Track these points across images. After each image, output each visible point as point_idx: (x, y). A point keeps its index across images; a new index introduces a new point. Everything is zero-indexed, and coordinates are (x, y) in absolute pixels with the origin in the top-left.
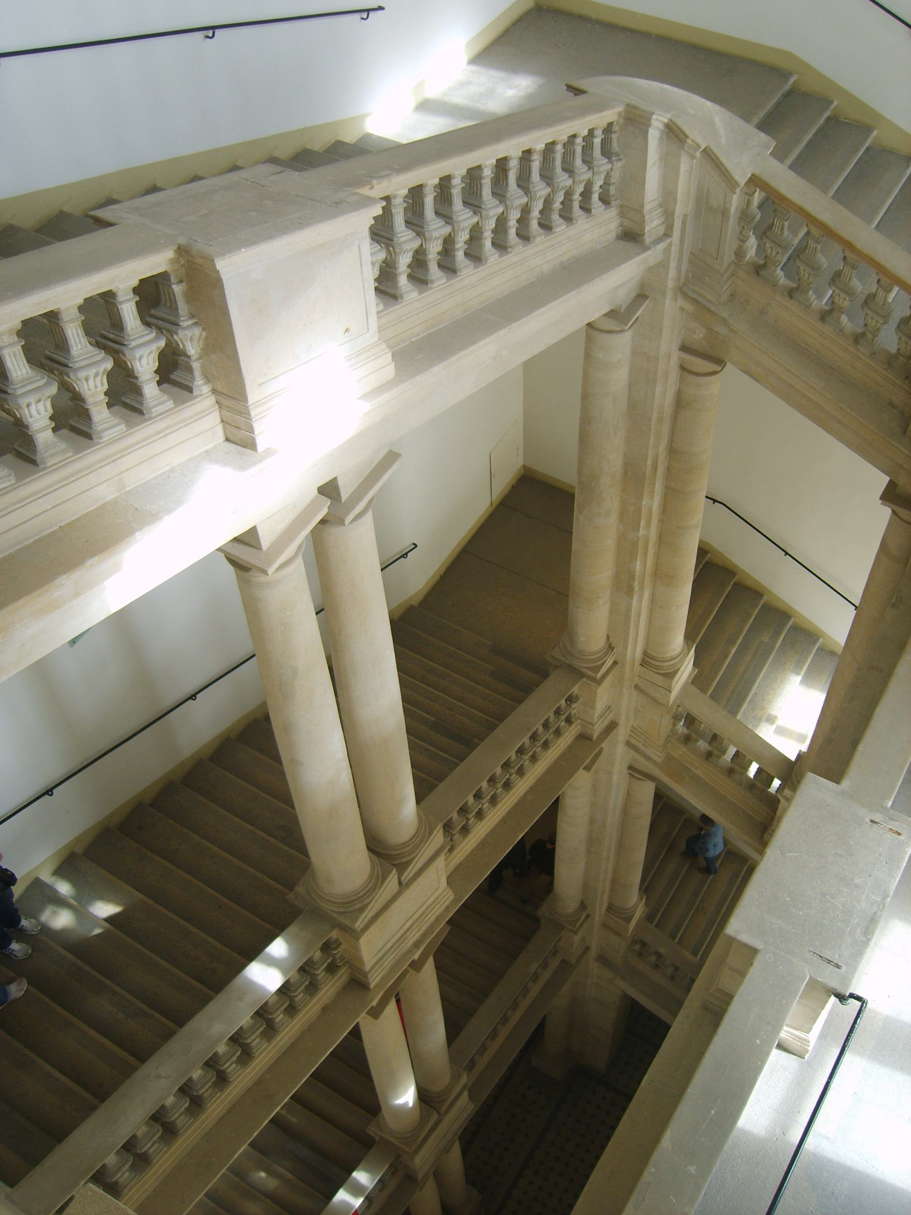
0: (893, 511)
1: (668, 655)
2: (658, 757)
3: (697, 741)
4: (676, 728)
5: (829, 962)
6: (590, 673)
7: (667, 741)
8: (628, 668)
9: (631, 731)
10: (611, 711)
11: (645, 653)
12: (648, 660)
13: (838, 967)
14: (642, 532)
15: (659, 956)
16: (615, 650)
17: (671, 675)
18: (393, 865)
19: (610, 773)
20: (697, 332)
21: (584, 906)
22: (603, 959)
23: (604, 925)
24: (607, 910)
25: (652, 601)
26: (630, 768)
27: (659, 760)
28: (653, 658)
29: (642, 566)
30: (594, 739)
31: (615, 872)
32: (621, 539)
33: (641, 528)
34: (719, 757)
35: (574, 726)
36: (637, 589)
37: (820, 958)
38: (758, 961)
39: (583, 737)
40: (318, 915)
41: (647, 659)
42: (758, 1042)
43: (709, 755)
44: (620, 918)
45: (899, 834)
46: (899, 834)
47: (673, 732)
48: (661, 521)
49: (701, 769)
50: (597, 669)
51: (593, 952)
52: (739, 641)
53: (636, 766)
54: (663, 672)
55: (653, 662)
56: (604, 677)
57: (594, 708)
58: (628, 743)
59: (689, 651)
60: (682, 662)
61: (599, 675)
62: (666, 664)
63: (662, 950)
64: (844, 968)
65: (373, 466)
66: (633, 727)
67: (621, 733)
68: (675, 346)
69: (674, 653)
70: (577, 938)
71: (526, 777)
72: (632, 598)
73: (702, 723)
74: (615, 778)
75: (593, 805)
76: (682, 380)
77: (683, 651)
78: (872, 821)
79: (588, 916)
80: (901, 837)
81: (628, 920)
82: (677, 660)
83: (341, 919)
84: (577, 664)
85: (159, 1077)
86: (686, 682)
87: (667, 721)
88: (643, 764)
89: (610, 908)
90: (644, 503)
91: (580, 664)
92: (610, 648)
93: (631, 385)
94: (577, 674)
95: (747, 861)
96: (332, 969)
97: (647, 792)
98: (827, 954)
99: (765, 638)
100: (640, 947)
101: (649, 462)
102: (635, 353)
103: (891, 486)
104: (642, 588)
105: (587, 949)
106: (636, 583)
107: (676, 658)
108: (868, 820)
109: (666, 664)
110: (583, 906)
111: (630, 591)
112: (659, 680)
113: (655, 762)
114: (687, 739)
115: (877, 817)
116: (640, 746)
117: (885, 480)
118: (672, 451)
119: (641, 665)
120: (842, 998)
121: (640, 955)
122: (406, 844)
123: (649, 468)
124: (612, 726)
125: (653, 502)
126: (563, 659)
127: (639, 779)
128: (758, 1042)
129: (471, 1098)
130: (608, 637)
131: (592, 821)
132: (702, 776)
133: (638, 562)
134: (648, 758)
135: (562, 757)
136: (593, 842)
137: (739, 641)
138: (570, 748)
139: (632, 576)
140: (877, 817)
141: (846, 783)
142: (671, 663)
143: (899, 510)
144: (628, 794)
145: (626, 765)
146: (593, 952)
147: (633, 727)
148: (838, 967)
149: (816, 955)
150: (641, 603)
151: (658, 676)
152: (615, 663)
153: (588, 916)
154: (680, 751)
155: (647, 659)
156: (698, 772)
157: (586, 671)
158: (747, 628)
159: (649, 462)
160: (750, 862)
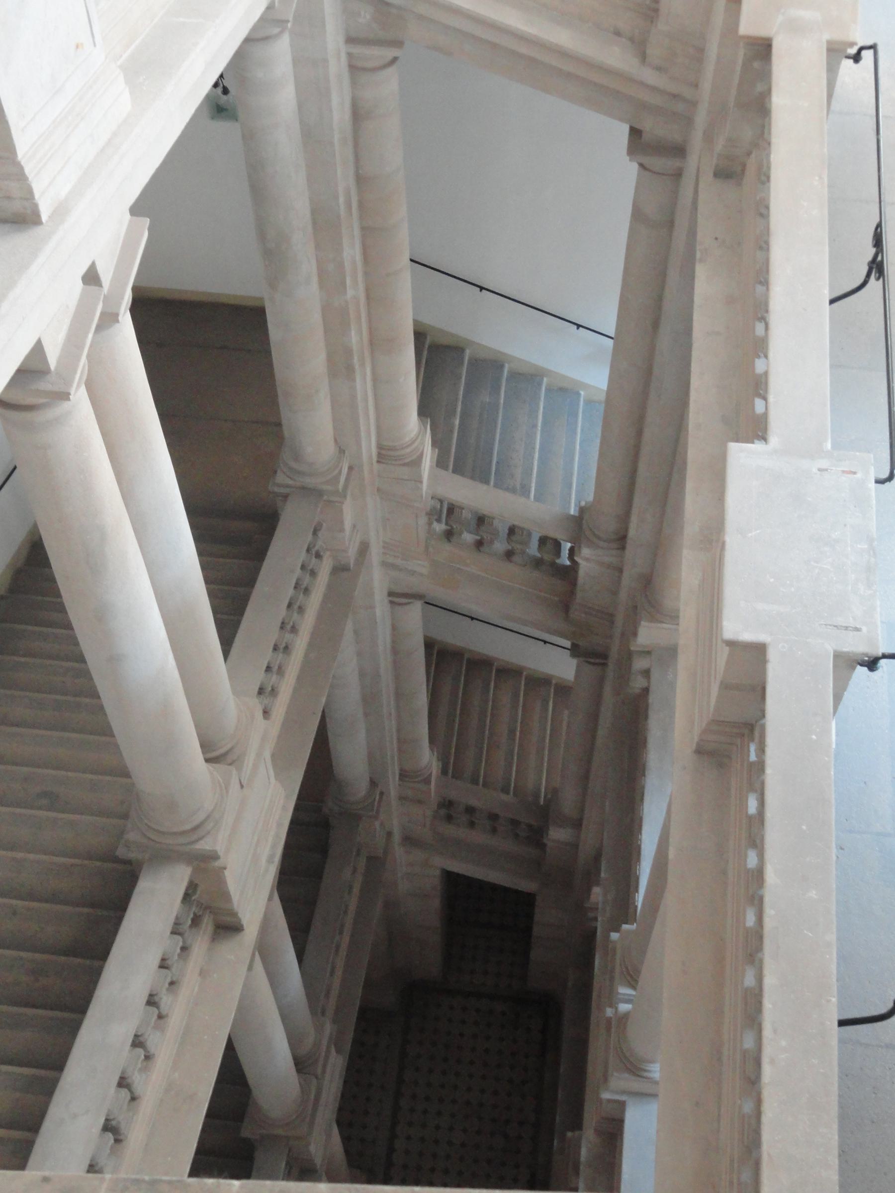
0: (641, 165)
1: (407, 439)
2: (422, 566)
3: (460, 534)
4: (433, 526)
5: (846, 628)
7: (427, 547)
8: (366, 469)
9: (384, 547)
10: (358, 531)
11: (380, 447)
12: (385, 455)
13: (857, 630)
14: (350, 293)
16: (346, 452)
17: (416, 463)
18: (230, 764)
19: (372, 607)
20: (363, 13)
21: (374, 782)
22: (409, 840)
23: (402, 798)
24: (400, 779)
25: (375, 380)
26: (391, 594)
27: (424, 571)
29: (356, 338)
30: (352, 566)
31: (399, 730)
32: (326, 309)
33: (348, 288)
34: (491, 542)
35: (325, 559)
36: (357, 367)
37: (835, 628)
38: (772, 655)
39: (339, 569)
42: (814, 737)
43: (479, 544)
44: (419, 782)
45: (855, 473)
46: (855, 473)
47: (430, 532)
48: (366, 274)
50: (337, 478)
51: (397, 837)
52: (459, 409)
54: (407, 461)
55: (391, 453)
56: (346, 487)
57: (342, 530)
58: (384, 564)
59: (426, 429)
60: (423, 443)
61: (341, 486)
62: (408, 450)
64: (864, 629)
65: (121, 241)
66: (384, 542)
67: (375, 554)
68: (341, 39)
69: (413, 434)
70: (377, 824)
71: (301, 633)
72: (354, 380)
73: (463, 509)
74: (378, 612)
75: (359, 654)
76: (354, 83)
77: (421, 429)
78: (820, 470)
79: (382, 794)
80: (859, 475)
81: (427, 781)
82: (419, 440)
84: (309, 481)
86: (431, 467)
87: (423, 520)
89: (404, 775)
90: (345, 254)
92: (342, 451)
93: (300, 106)
94: (312, 493)
96: (196, 922)
98: (840, 621)
101: (341, 200)
102: (297, 62)
103: (635, 133)
104: (363, 365)
105: (389, 834)
106: (356, 360)
107: (415, 440)
108: (815, 470)
109: (408, 450)
110: (373, 783)
111: (350, 370)
113: (421, 575)
114: (449, 535)
115: (824, 463)
116: (399, 562)
117: (626, 128)
118: (361, 180)
120: (872, 664)
121: (449, 818)
123: (342, 207)
124: (364, 549)
125: (352, 252)
126: (291, 482)
127: (406, 604)
128: (814, 737)
129: (338, 1051)
130: (336, 441)
131: (362, 674)
132: (479, 573)
133: (353, 333)
134: (413, 573)
135: (326, 598)
136: (370, 699)
137: (459, 409)
138: (330, 587)
139: (349, 352)
140: (824, 463)
141: (774, 440)
143: (647, 160)
144: (394, 628)
145: (385, 593)
146: (397, 837)
148: (857, 630)
149: (829, 627)
150: (363, 384)
152: (351, 468)
153: (382, 794)
154: (447, 549)
155: (383, 452)
157: (325, 487)
158: (461, 393)
159: (341, 200)
160: (525, 673)
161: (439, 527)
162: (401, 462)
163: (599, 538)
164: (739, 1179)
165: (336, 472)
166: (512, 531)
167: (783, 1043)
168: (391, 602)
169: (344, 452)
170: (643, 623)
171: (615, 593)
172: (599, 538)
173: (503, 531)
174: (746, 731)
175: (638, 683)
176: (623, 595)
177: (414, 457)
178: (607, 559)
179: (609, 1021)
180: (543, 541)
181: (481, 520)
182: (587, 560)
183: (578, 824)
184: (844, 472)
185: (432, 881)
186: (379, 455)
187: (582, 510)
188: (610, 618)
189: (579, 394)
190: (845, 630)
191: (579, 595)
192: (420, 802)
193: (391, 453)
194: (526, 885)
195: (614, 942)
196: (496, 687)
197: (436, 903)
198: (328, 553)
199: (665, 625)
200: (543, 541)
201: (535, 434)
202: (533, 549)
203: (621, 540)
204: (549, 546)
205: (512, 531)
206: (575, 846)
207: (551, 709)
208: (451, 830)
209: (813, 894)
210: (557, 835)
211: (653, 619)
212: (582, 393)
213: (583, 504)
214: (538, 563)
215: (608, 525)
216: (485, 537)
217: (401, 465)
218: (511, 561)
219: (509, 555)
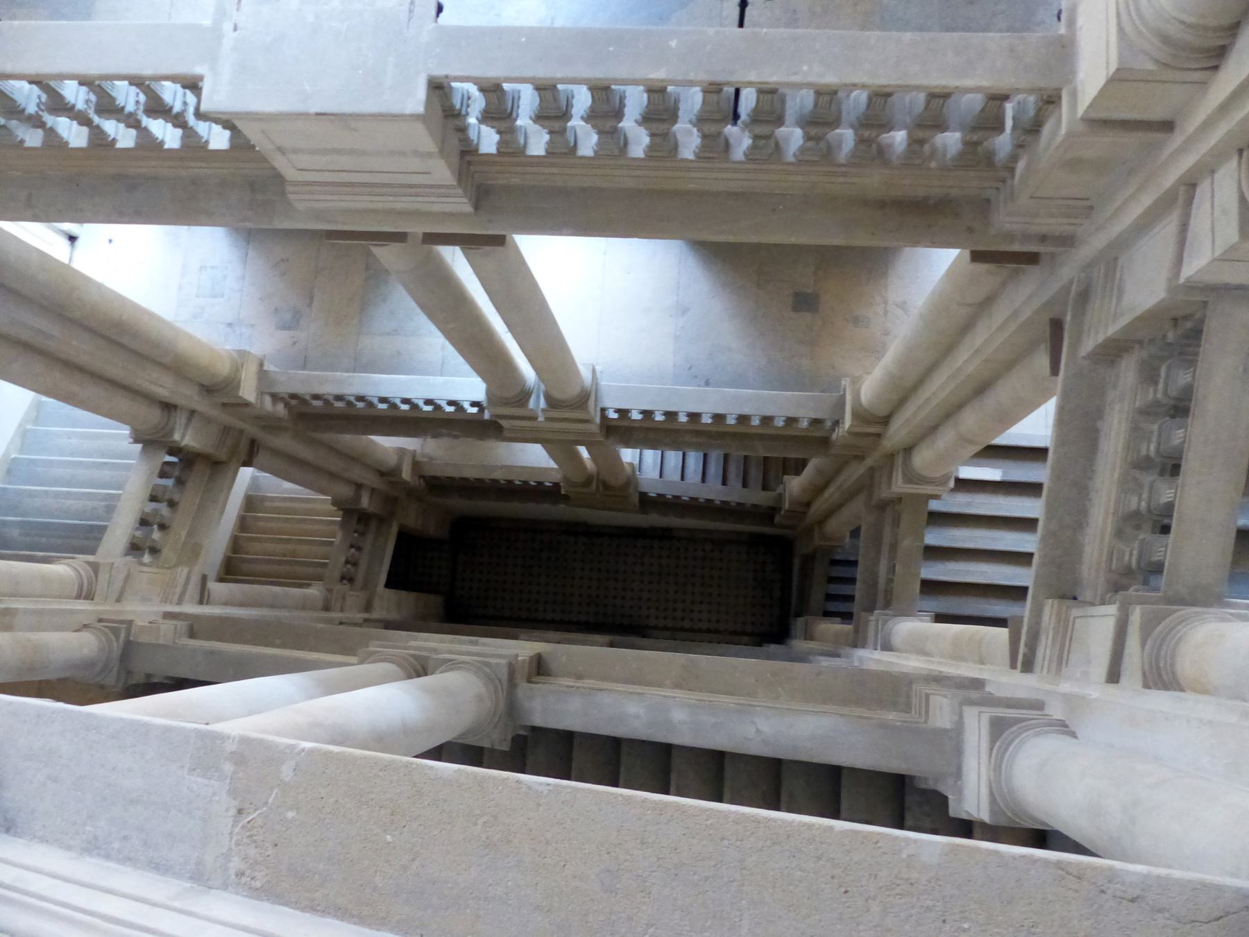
2: (182, 572)
3: (154, 540)
5: (411, 11)
6: (122, 635)
7: (163, 567)
9: (166, 602)
11: (78, 597)
12: (86, 593)
15: (347, 562)
22: (368, 607)
23: (342, 610)
26: (201, 602)
27: (186, 571)
28: (81, 587)
30: (190, 622)
39: (192, 634)
40: (512, 708)
41: (84, 594)
42: (523, 39)
43: (162, 527)
49: (180, 531)
51: (366, 615)
53: (197, 597)
54: (92, 574)
55: (85, 589)
56: (122, 622)
58: (180, 602)
63: (343, 559)
66: (161, 602)
72: (17, 609)
78: (235, 29)
83: (505, 678)
85: (758, 731)
88: (193, 588)
89: (327, 608)
91: (116, 649)
95: (236, 535)
97: (216, 588)
99: (15, 533)
100: (347, 578)
108: (236, 34)
112: (103, 576)
113: (189, 573)
114: (154, 551)
115: (227, 27)
116: (178, 590)
119: (92, 599)
122: (400, 665)
126: (115, 669)
128: (523, 39)
134: (188, 579)
142: (80, 570)
146: (366, 615)
147: (161, 602)
151: (99, 579)
155: (84, 594)
156: (184, 534)
161: (147, 558)
162: (94, 579)
163: (167, 424)
164: (844, 165)
165: (106, 630)
166: (153, 498)
167: (805, 68)
168: (207, 604)
169: (85, 625)
170: (241, 394)
171: (209, 420)
172: (167, 424)
173: (154, 505)
174: (468, 158)
175: (280, 409)
176: (214, 413)
177: (88, 568)
178: (183, 421)
179: (547, 419)
180: (163, 475)
181: (144, 522)
182: (183, 436)
183: (359, 487)
184: (238, 10)
185: (391, 593)
186: (87, 598)
187: (136, 441)
188: (226, 430)
189: (14, 459)
190: (413, 12)
191: (209, 450)
192: (344, 598)
193: (85, 589)
194: (394, 530)
195: (491, 416)
196: (247, 554)
197: (404, 594)
198: (177, 641)
199: (243, 377)
200: (163, 475)
201: (53, 491)
202: (169, 482)
203: (168, 407)
204: (167, 469)
205: (153, 498)
206: (373, 490)
207: (262, 515)
208: (360, 577)
209: (673, 44)
210: (365, 502)
211: (238, 387)
212: (13, 456)
213: (131, 440)
214: (180, 482)
215: (154, 416)
216: (159, 520)
217: (96, 580)
218: (178, 503)
219: (172, 504)
